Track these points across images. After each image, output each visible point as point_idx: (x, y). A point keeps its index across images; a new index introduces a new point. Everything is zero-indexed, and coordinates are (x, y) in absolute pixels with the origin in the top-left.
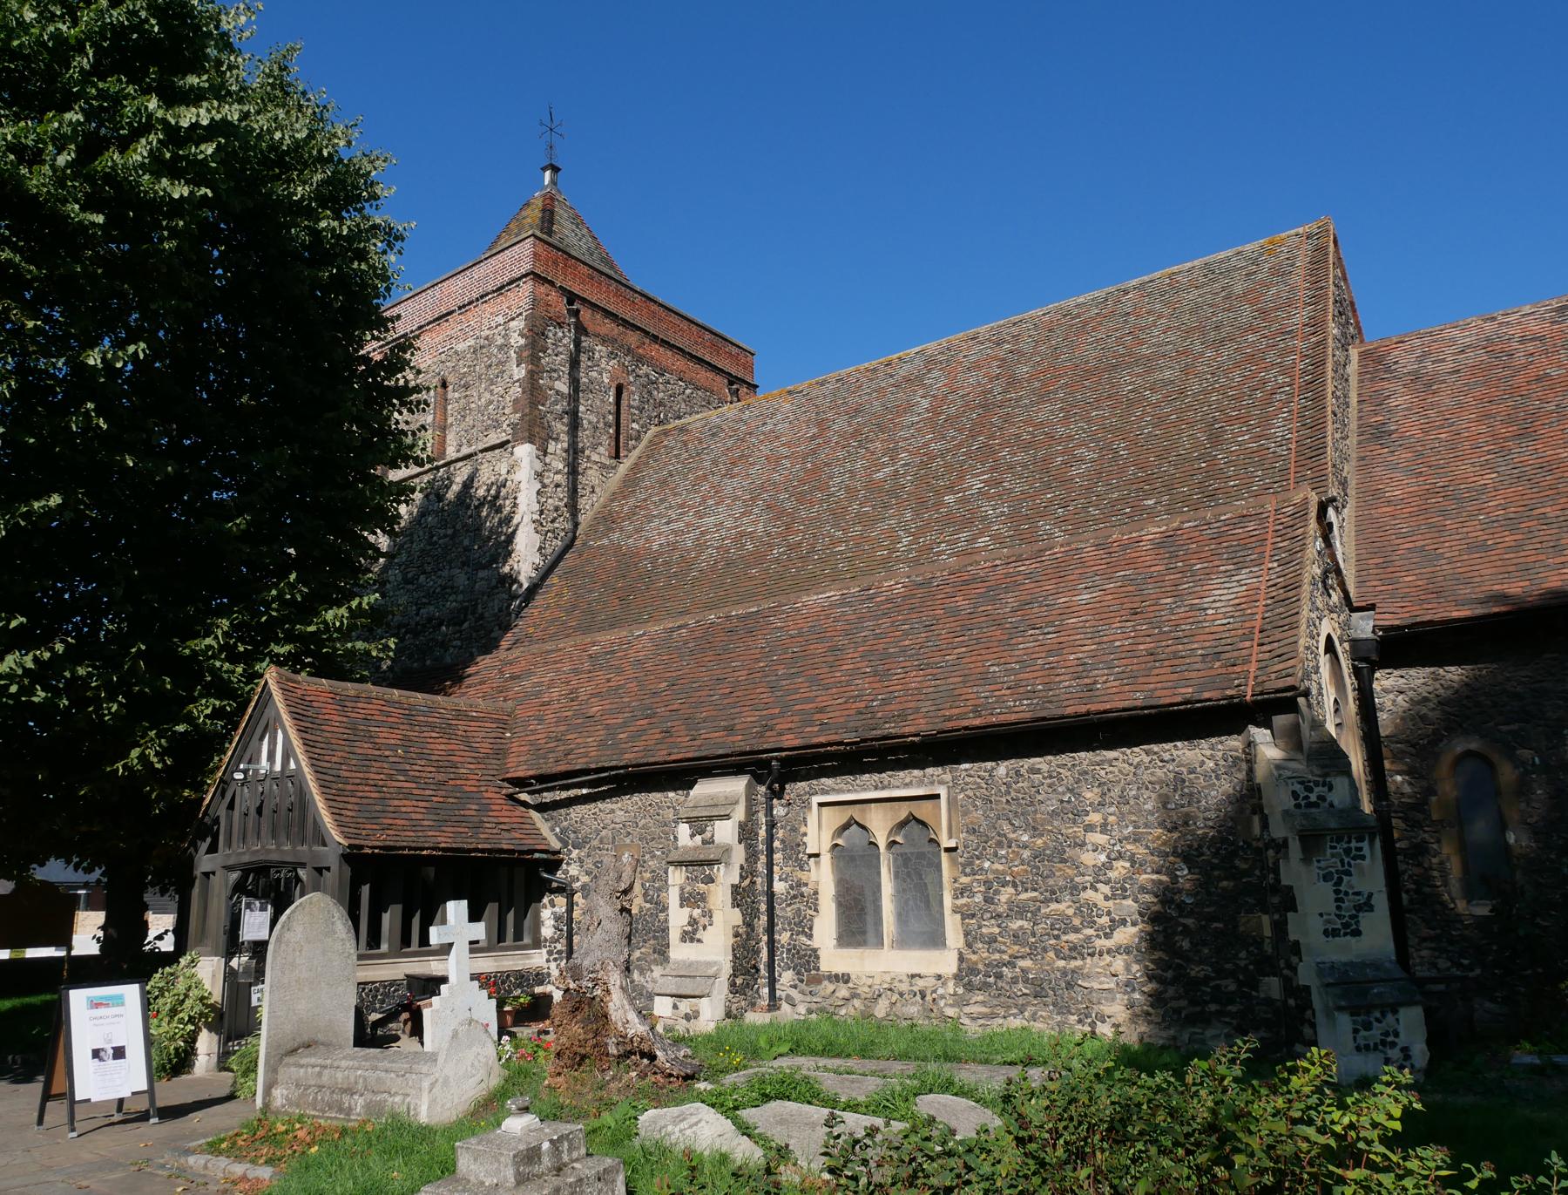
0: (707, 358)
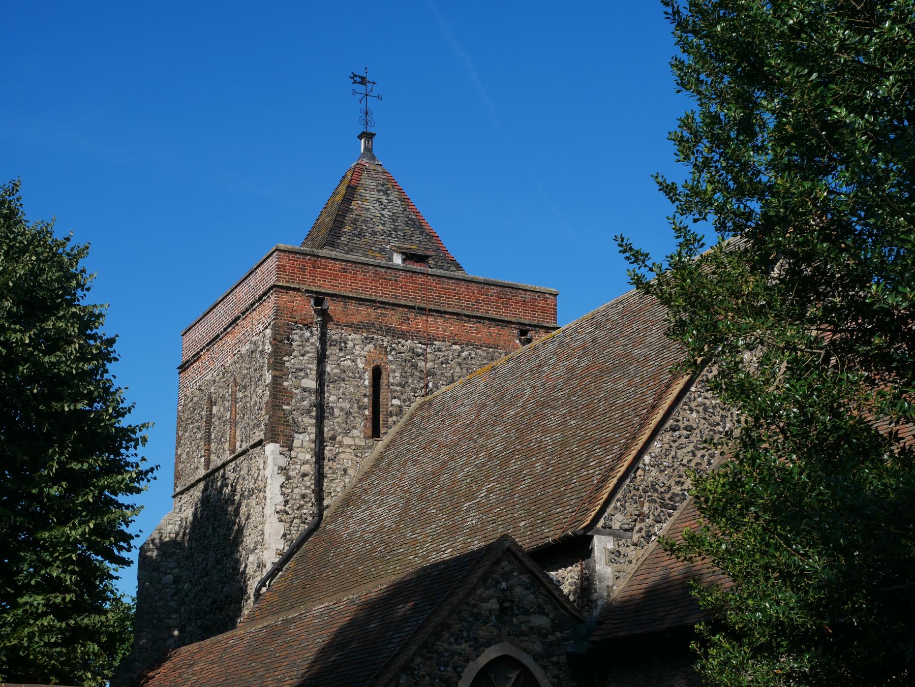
0: (492, 314)
